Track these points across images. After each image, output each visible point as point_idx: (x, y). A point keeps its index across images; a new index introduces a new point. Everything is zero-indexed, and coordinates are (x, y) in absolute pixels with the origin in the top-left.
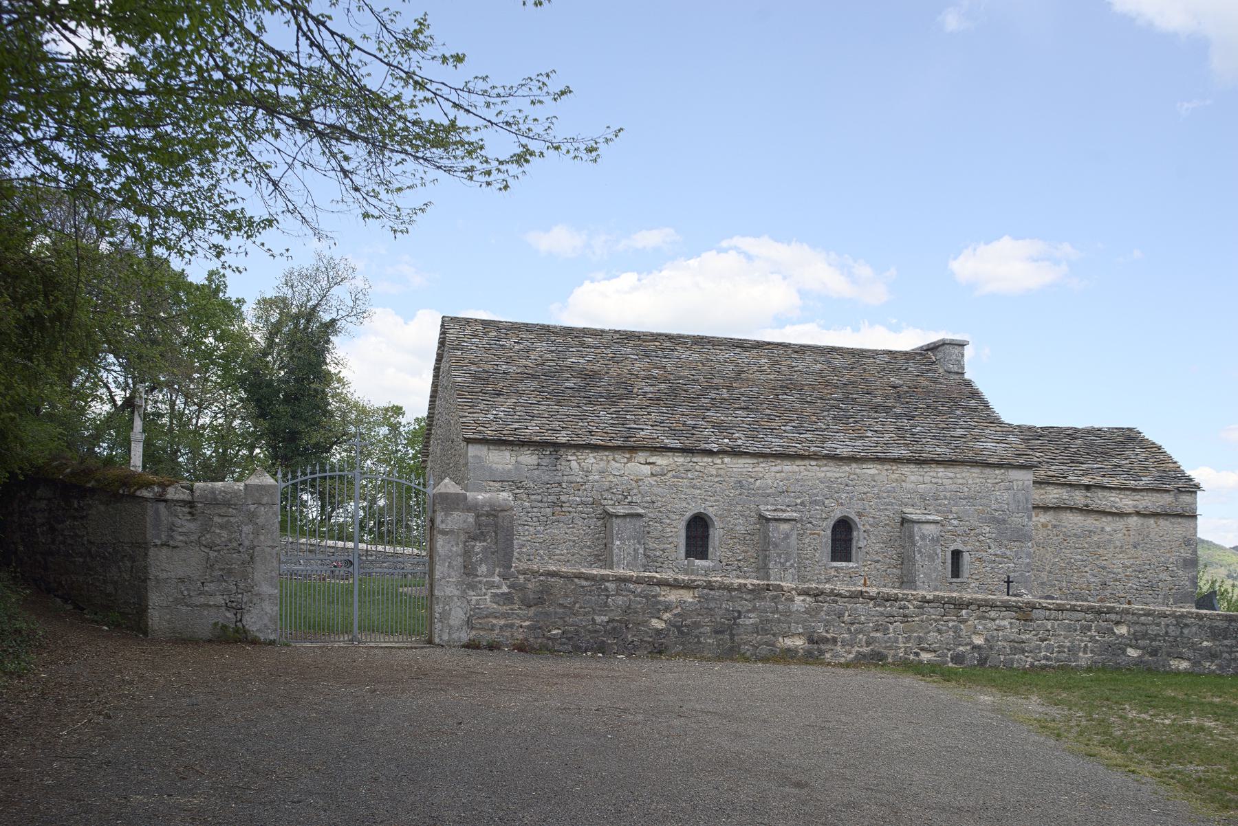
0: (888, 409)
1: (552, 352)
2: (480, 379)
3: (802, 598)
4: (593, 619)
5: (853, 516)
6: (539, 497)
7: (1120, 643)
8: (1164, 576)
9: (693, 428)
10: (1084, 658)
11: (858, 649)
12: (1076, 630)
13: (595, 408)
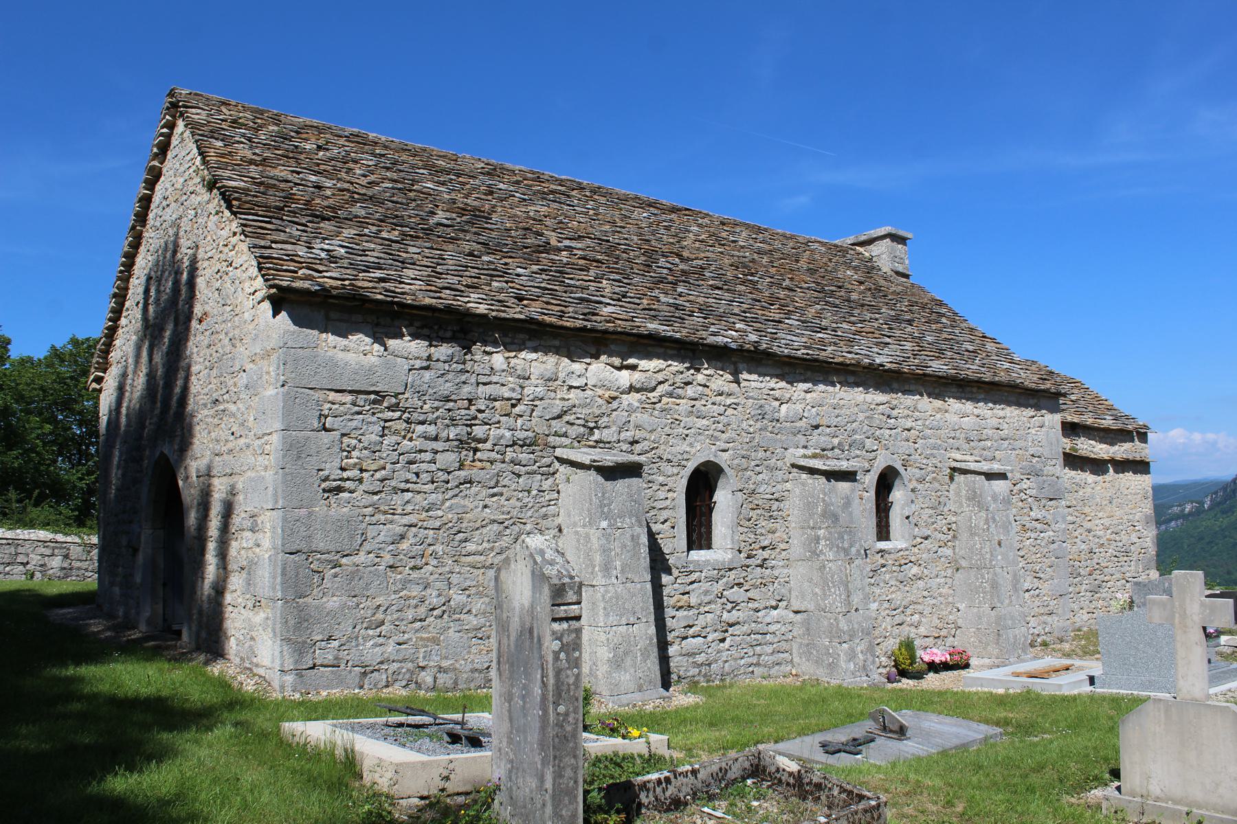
5: (898, 466)
6: (431, 429)
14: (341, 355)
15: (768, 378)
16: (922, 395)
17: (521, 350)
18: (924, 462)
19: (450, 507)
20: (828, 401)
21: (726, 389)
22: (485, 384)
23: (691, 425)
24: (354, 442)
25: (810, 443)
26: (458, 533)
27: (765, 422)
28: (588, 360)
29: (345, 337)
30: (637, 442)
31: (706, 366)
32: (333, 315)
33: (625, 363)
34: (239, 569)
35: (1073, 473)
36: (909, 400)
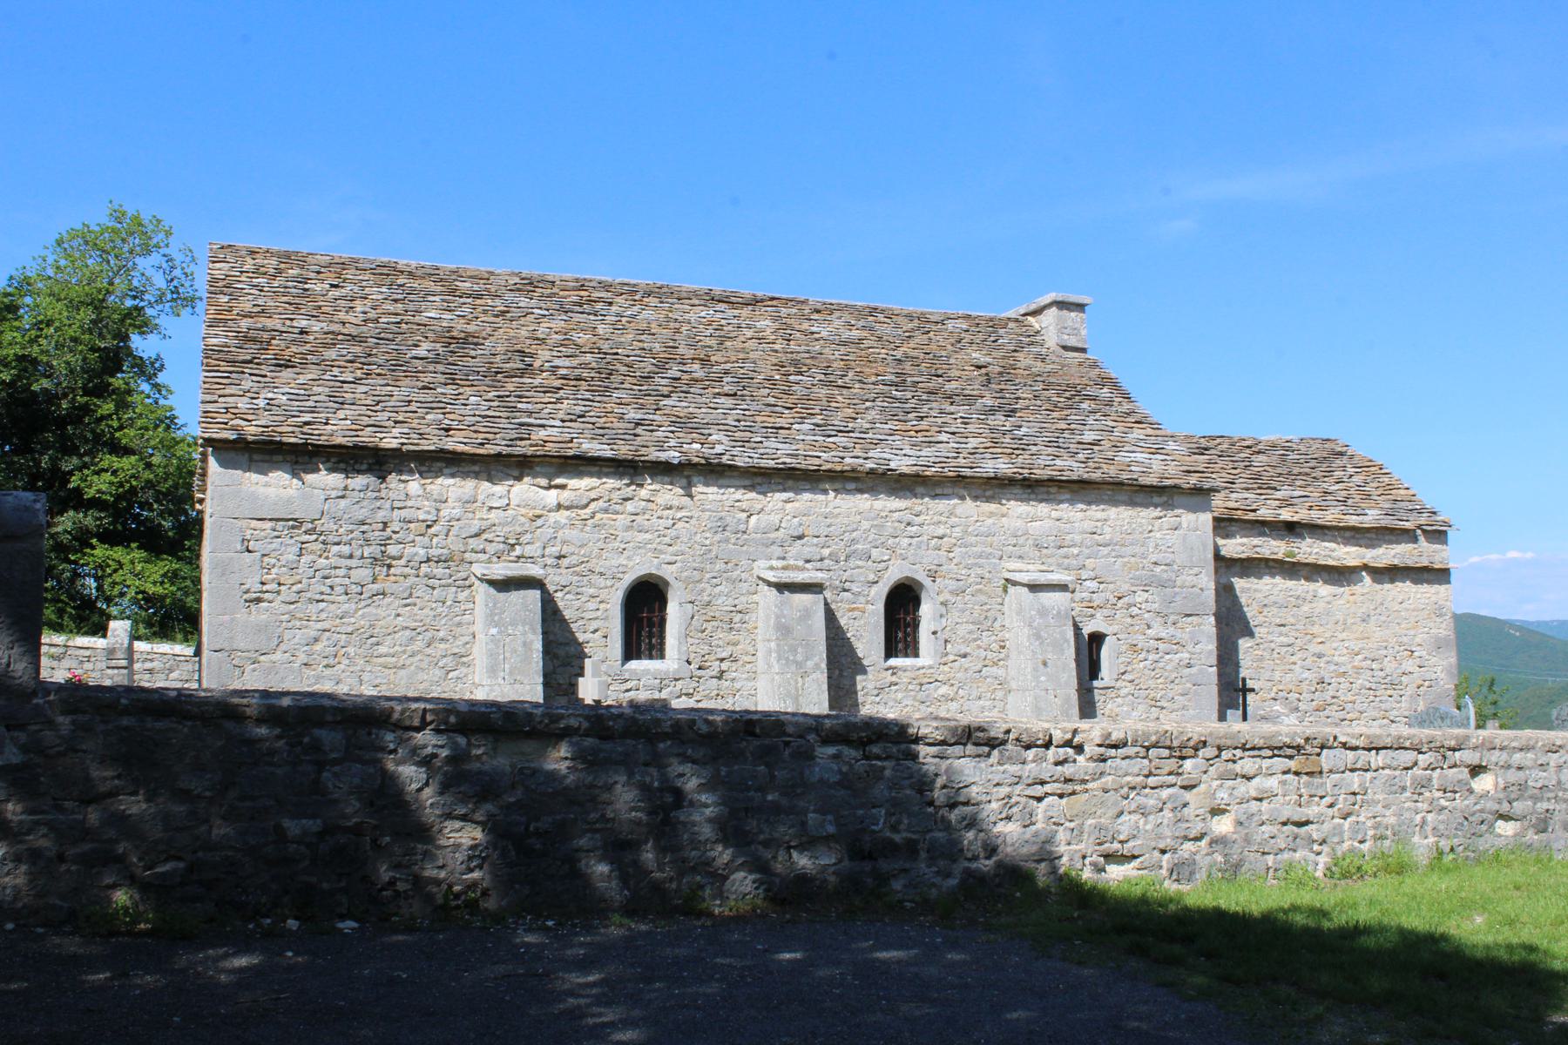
0: (970, 399)
1: (396, 301)
2: (254, 340)
3: (831, 750)
4: (279, 830)
5: (921, 577)
6: (346, 549)
7: (1482, 811)
8: (1409, 665)
9: (637, 424)
10: (1422, 845)
11: (966, 864)
12: (1404, 789)
13: (461, 390)
14: (262, 490)
15: (732, 490)
16: (962, 498)
17: (437, 477)
18: (963, 572)
19: (363, 616)
20: (817, 510)
21: (676, 503)
22: (399, 508)
23: (629, 539)
24: (273, 561)
25: (790, 554)
26: (372, 638)
27: (726, 533)
28: (511, 483)
29: (266, 474)
30: (564, 557)
31: (649, 481)
32: (256, 457)
33: (553, 483)
35: (1291, 584)
36: (942, 505)
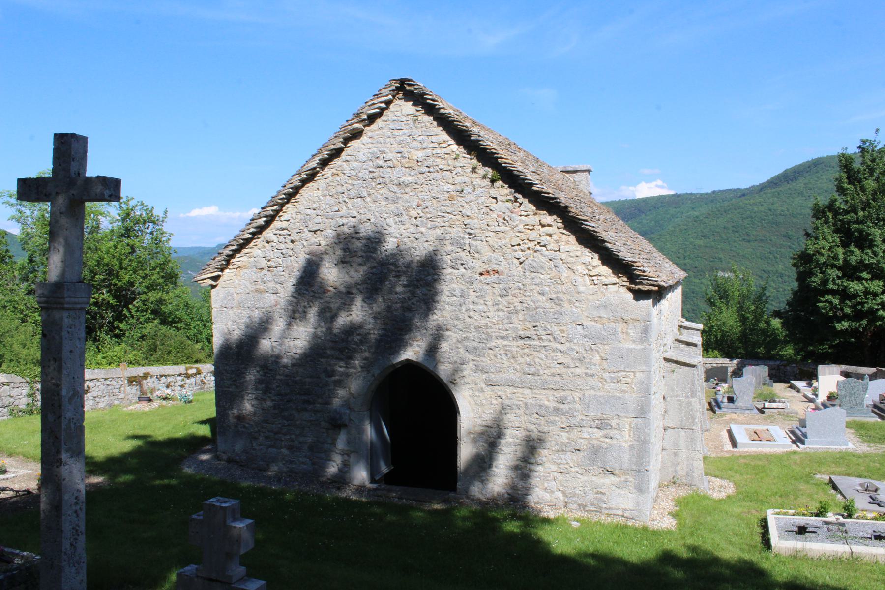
34: (574, 451)
